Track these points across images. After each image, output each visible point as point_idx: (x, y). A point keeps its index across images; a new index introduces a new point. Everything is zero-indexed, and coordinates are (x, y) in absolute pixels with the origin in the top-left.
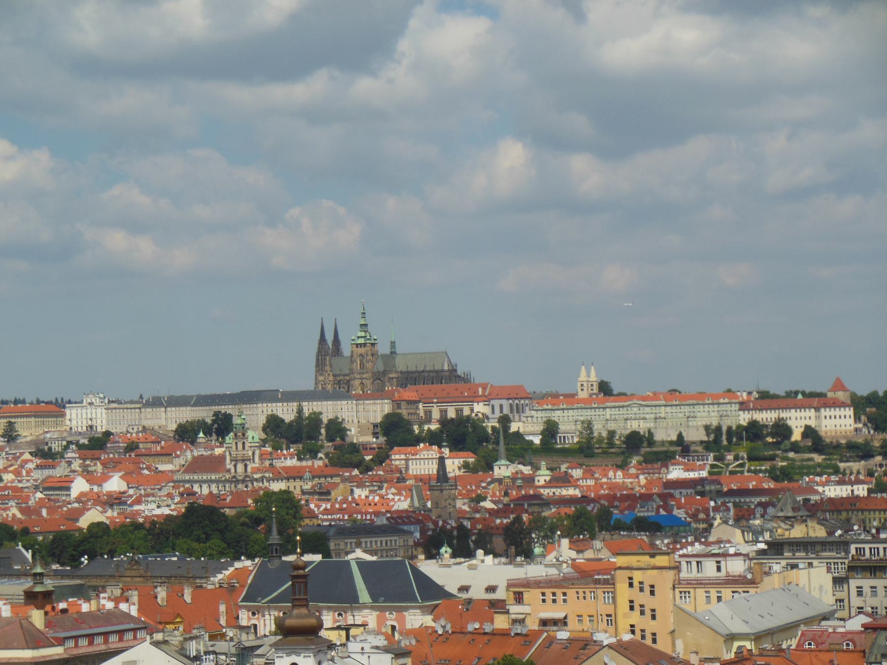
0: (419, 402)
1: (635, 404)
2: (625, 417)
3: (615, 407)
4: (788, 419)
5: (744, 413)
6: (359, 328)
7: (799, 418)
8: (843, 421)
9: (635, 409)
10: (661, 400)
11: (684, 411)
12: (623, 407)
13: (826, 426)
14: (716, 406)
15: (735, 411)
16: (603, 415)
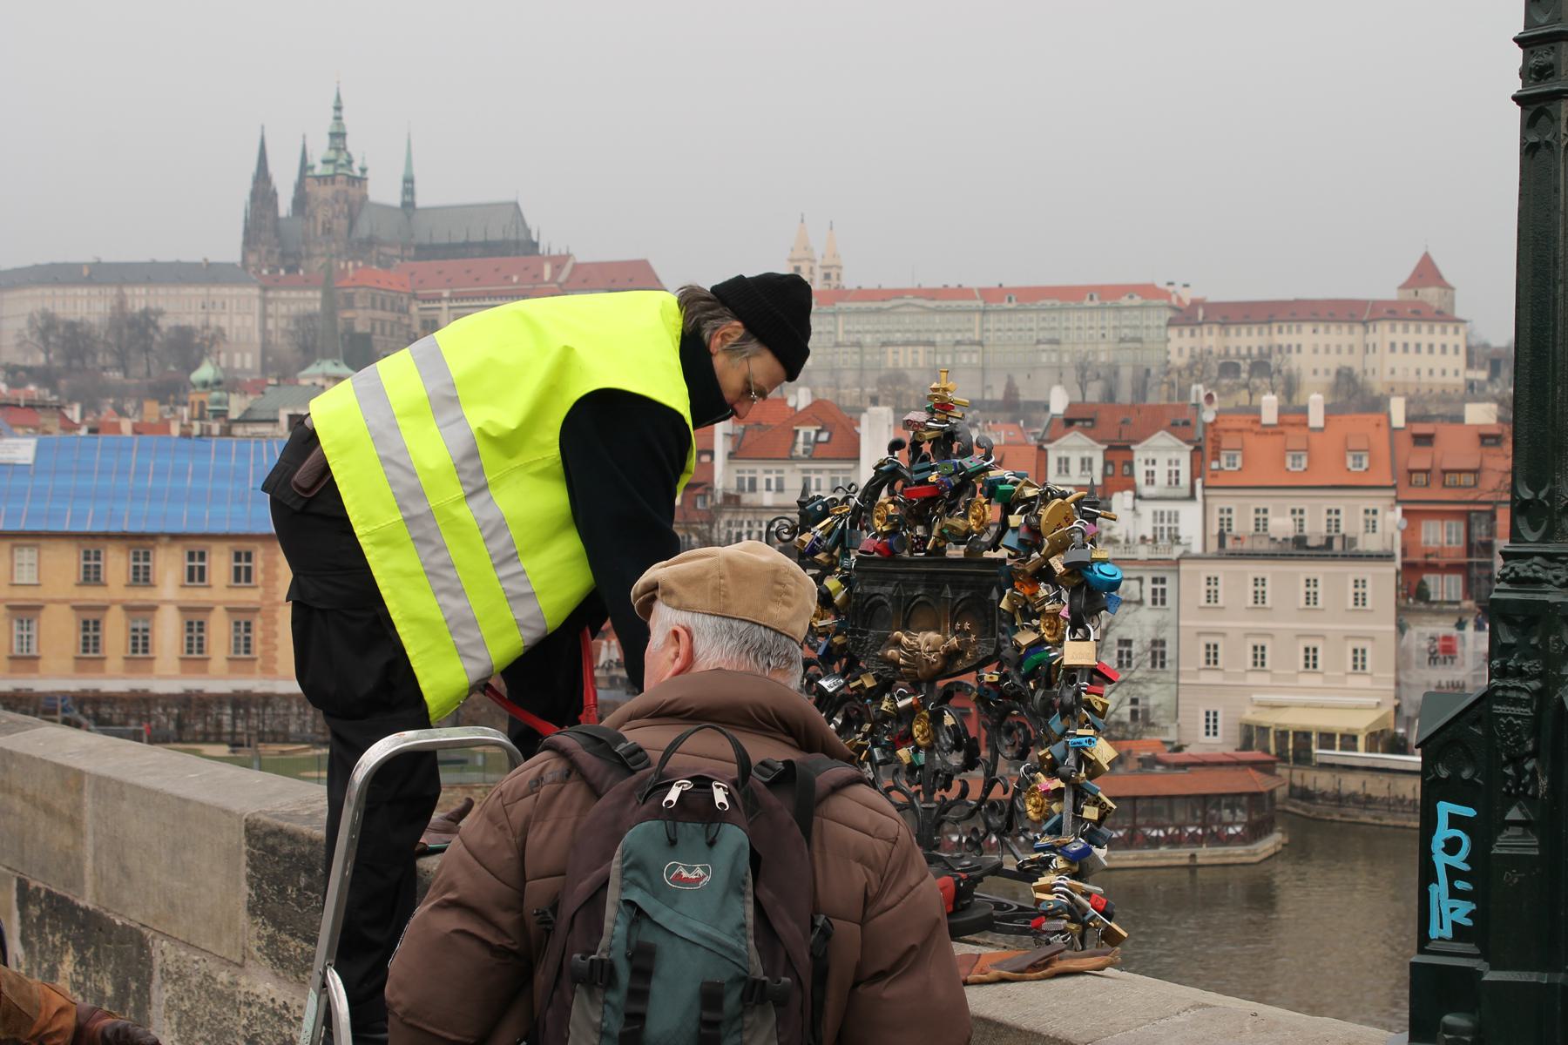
0: (415, 297)
1: (907, 305)
2: (883, 337)
3: (858, 312)
4: (1294, 349)
5: (1180, 334)
6: (326, 140)
7: (1321, 350)
8: (1437, 361)
9: (907, 319)
10: (974, 298)
11: (1029, 325)
12: (878, 311)
13: (1393, 372)
14: (1109, 315)
15: (1159, 327)
16: (830, 332)
